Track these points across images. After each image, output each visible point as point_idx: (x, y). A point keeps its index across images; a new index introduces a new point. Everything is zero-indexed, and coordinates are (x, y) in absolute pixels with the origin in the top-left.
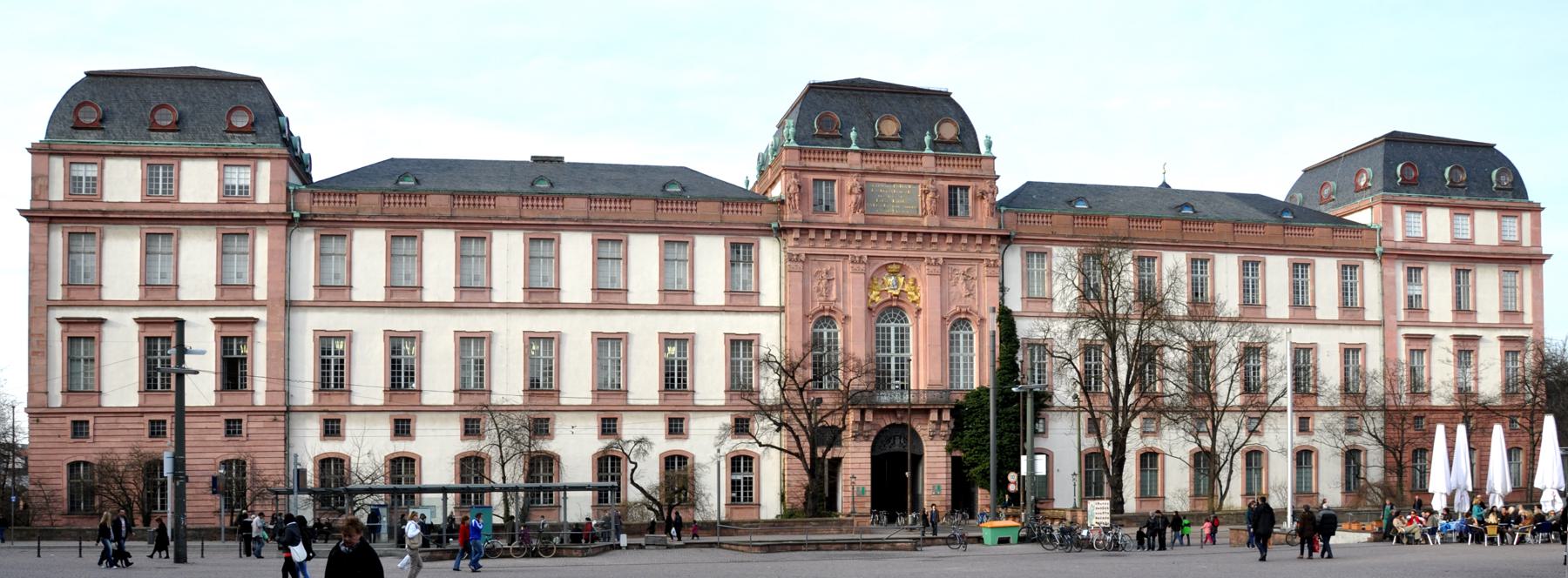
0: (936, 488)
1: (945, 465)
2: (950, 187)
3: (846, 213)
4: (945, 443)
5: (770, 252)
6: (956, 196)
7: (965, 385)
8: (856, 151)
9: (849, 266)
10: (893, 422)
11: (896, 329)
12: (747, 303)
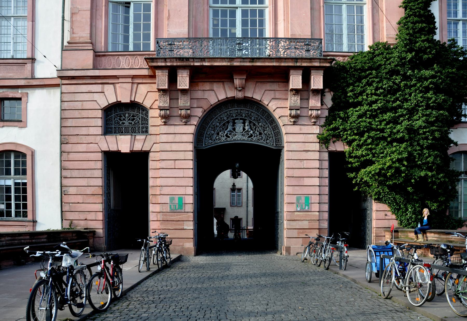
0: (303, 200)
1: (316, 164)
4: (316, 130)
7: (350, 46)
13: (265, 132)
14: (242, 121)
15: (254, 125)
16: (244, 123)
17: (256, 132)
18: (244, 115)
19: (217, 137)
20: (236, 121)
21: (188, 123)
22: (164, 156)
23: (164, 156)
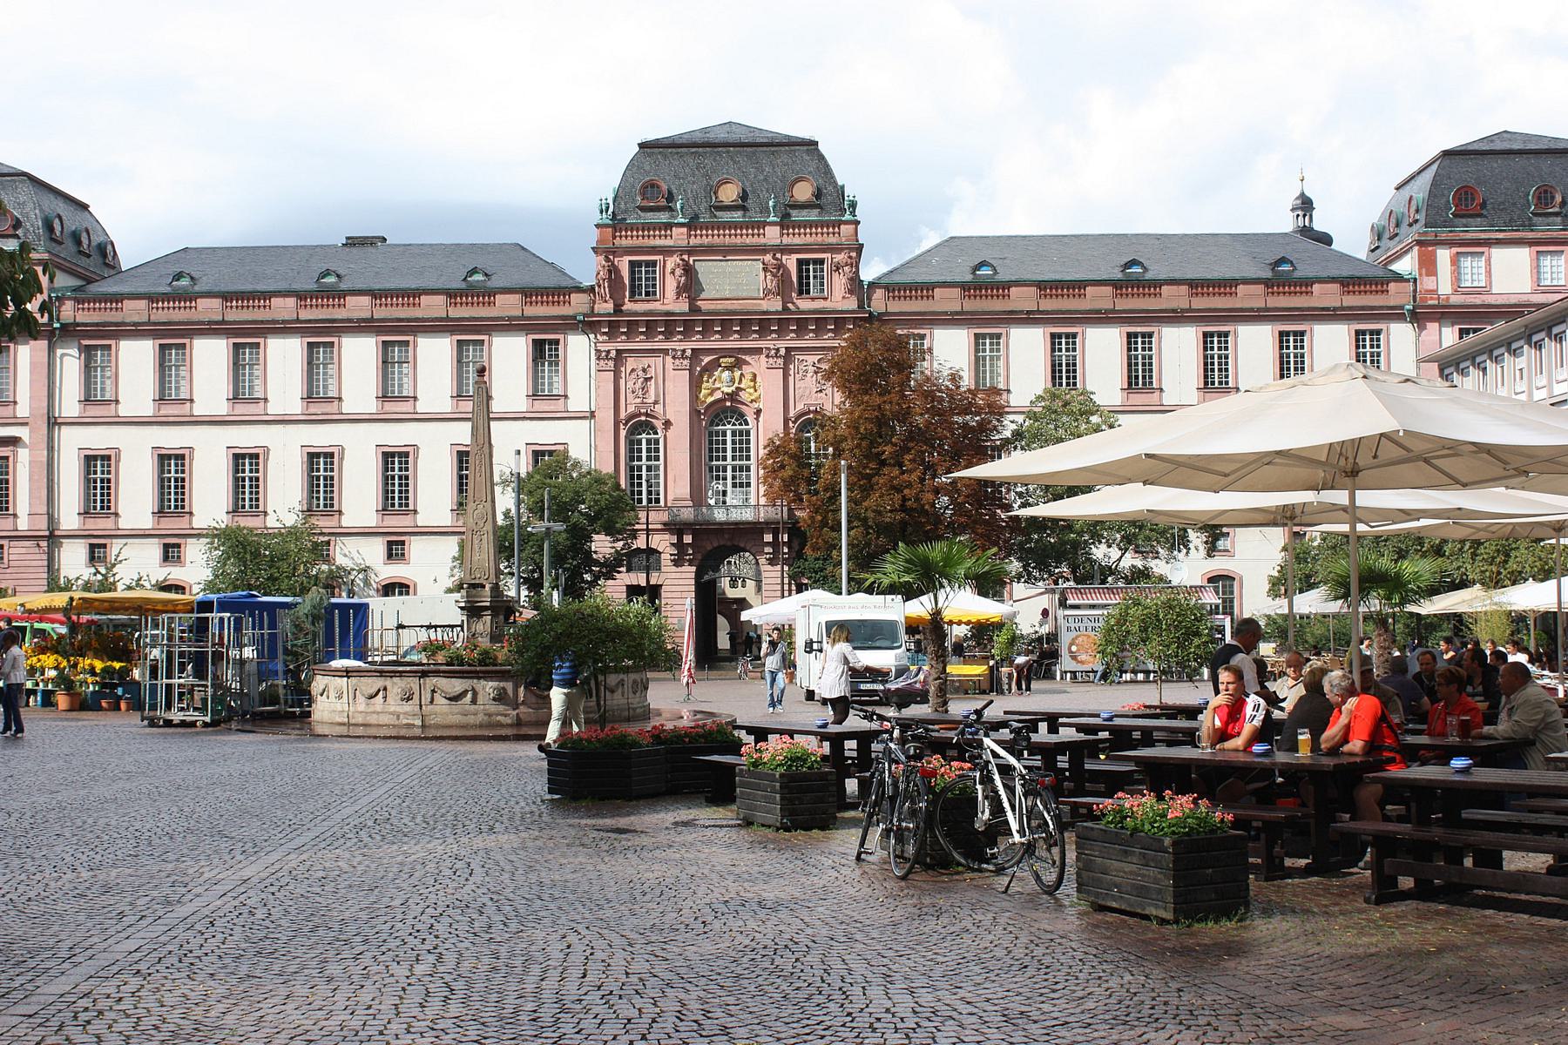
2: (800, 262)
3: (670, 300)
5: (578, 349)
6: (808, 271)
8: (681, 225)
9: (669, 359)
11: (734, 433)
12: (552, 408)
22: (674, 589)
23: (674, 589)
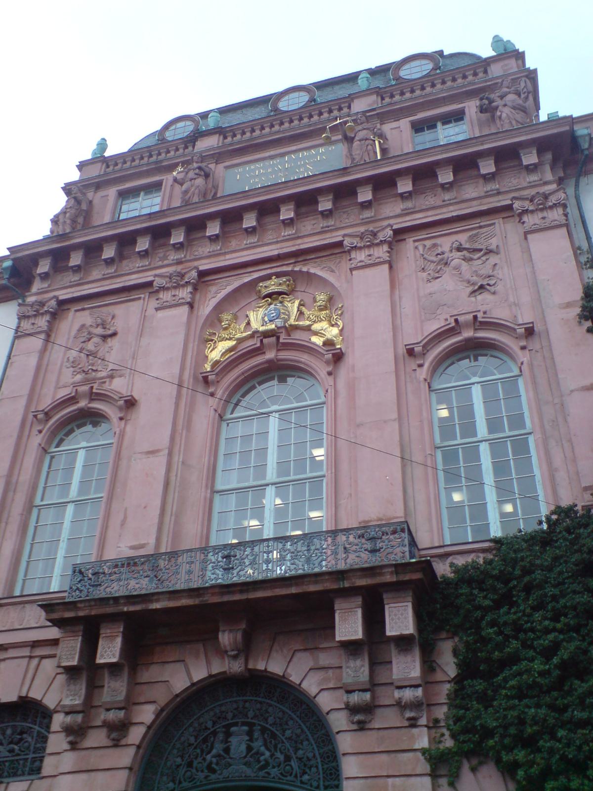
10: (218, 667)
13: (300, 752)
14: (245, 728)
15: (274, 736)
16: (250, 733)
17: (278, 754)
18: (251, 714)
19: (189, 774)
20: (233, 729)
21: (123, 742)
